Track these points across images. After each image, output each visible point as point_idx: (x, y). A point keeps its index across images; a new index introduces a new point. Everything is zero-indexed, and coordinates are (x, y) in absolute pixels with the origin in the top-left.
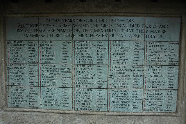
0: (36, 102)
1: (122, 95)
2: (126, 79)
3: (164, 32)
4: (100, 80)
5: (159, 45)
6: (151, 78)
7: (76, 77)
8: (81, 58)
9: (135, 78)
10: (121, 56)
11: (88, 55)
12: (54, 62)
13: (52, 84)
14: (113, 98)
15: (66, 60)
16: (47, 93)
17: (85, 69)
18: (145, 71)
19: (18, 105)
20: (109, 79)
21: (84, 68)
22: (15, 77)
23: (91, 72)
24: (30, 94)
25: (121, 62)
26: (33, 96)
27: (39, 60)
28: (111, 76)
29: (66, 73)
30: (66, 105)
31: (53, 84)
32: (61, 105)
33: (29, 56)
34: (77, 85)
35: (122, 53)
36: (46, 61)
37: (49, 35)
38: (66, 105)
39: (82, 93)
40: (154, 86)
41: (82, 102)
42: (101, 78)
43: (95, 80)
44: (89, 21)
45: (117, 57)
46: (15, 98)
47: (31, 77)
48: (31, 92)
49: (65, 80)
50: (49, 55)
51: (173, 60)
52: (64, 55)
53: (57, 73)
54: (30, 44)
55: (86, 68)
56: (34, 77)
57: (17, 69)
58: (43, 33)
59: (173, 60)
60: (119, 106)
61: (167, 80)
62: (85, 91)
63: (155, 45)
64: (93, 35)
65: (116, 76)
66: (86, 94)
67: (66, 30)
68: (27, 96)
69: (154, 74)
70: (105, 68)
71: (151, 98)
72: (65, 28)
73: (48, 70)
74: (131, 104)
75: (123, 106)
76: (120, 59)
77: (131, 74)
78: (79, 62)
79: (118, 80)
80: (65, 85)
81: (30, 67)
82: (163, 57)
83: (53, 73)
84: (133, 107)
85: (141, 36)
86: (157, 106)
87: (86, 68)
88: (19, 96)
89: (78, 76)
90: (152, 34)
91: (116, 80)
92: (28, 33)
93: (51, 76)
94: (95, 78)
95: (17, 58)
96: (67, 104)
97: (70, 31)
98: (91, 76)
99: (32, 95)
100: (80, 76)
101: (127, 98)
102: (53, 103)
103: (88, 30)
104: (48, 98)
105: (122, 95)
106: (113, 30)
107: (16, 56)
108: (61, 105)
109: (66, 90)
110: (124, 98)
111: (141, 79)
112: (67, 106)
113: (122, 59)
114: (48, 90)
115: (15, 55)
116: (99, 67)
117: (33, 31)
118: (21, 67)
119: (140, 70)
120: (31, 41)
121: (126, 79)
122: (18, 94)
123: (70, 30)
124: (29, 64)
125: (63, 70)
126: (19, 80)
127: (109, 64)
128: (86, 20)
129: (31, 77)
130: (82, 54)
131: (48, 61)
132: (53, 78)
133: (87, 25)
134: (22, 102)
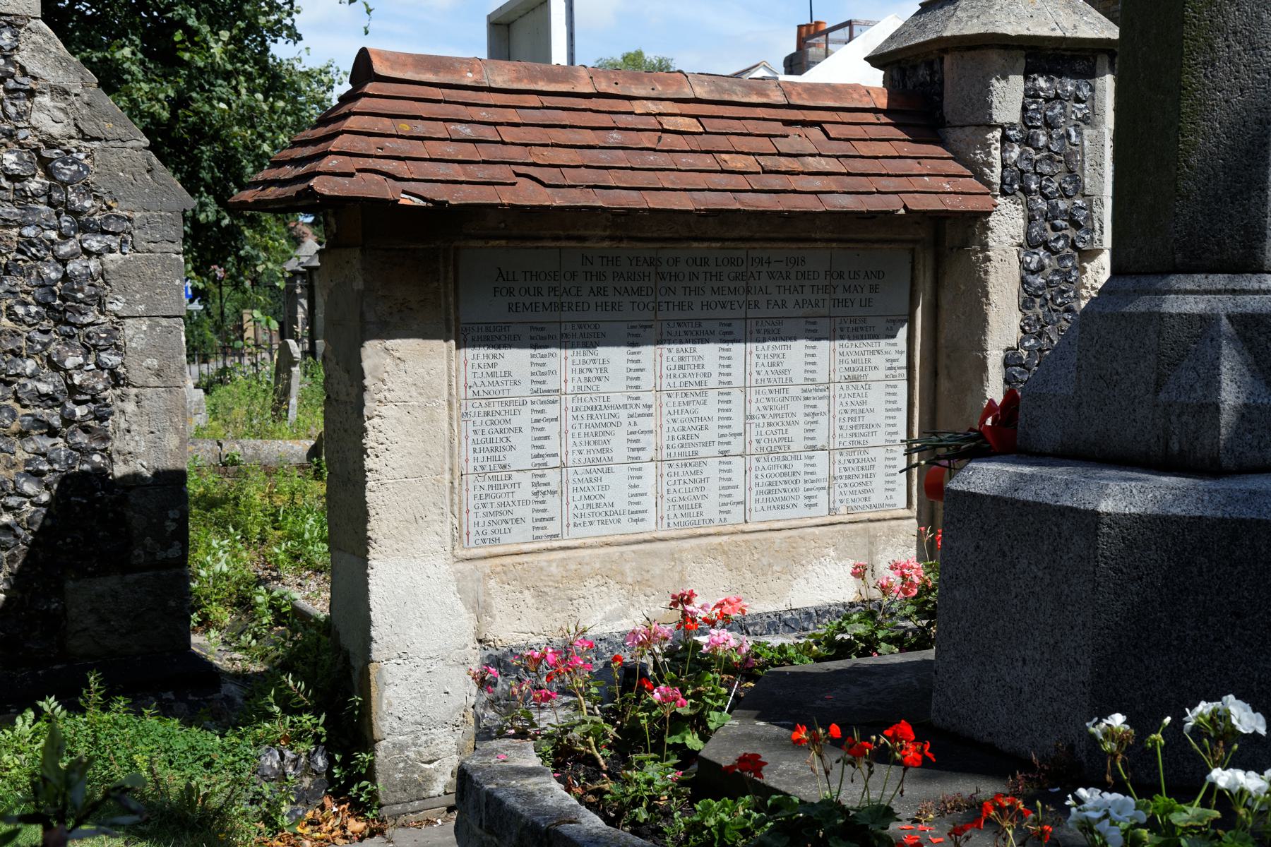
0: (552, 519)
1: (780, 471)
2: (789, 423)
3: (874, 289)
4: (726, 431)
5: (864, 325)
6: (846, 416)
7: (665, 429)
8: (677, 372)
9: (809, 419)
10: (776, 360)
11: (696, 363)
12: (604, 386)
13: (599, 456)
14: (758, 481)
15: (638, 378)
16: (586, 484)
17: (688, 403)
18: (832, 399)
19: (497, 536)
20: (748, 426)
21: (685, 400)
22: (489, 446)
23: (703, 411)
24: (536, 494)
25: (777, 376)
26: (543, 502)
27: (563, 384)
28: (752, 417)
29: (638, 420)
30: (640, 516)
31: (602, 455)
32: (627, 516)
33: (533, 374)
34: (669, 451)
35: (777, 352)
36: (583, 384)
37: (593, 306)
38: (640, 516)
39: (680, 473)
40: (854, 439)
41: (682, 503)
42: (729, 427)
43: (710, 435)
44: (698, 263)
45: (766, 364)
46: (486, 515)
47: (539, 438)
48: (539, 488)
49: (637, 441)
50: (592, 366)
51: (895, 365)
52: (633, 366)
53: (614, 420)
54: (534, 333)
55: (692, 398)
56: (547, 438)
57: (493, 418)
58: (574, 300)
59: (895, 365)
60: (772, 504)
61: (883, 422)
62: (689, 469)
63: (855, 326)
64: (708, 305)
65: (764, 416)
66: (691, 477)
67: (639, 291)
68: (524, 502)
69: (853, 407)
70: (737, 396)
71: (848, 473)
72: (636, 285)
73: (589, 412)
74: (802, 493)
75: (783, 503)
76: (773, 369)
77: (798, 408)
78: (672, 385)
79: (770, 428)
80: (635, 454)
81: (537, 407)
82: (871, 357)
83: (603, 421)
84: (807, 502)
85: (821, 304)
86: (864, 496)
87: (692, 398)
88: (500, 505)
89: (672, 425)
90: (847, 295)
91: (764, 430)
92: (528, 300)
93: (598, 430)
94: (713, 425)
95: (495, 379)
96: (642, 512)
97: (650, 293)
98: (705, 423)
99: (540, 498)
100: (676, 426)
101: (793, 478)
102: (603, 514)
103: (697, 291)
104: (588, 502)
105: (780, 471)
106: (758, 289)
107: (493, 374)
108: (624, 519)
109: (640, 469)
110: (784, 479)
111: (823, 420)
112: (642, 520)
113: (778, 368)
114: (588, 476)
115: (490, 370)
116: (723, 394)
117: (545, 292)
118: (507, 408)
119: (820, 398)
120: (539, 326)
121: (789, 423)
122: (496, 500)
123: (650, 290)
124: (534, 399)
125: (631, 411)
126: (502, 454)
127: (748, 385)
128: (690, 261)
129: (539, 438)
130: (681, 359)
131: (589, 384)
132: (603, 438)
133: (694, 276)
134: (509, 525)
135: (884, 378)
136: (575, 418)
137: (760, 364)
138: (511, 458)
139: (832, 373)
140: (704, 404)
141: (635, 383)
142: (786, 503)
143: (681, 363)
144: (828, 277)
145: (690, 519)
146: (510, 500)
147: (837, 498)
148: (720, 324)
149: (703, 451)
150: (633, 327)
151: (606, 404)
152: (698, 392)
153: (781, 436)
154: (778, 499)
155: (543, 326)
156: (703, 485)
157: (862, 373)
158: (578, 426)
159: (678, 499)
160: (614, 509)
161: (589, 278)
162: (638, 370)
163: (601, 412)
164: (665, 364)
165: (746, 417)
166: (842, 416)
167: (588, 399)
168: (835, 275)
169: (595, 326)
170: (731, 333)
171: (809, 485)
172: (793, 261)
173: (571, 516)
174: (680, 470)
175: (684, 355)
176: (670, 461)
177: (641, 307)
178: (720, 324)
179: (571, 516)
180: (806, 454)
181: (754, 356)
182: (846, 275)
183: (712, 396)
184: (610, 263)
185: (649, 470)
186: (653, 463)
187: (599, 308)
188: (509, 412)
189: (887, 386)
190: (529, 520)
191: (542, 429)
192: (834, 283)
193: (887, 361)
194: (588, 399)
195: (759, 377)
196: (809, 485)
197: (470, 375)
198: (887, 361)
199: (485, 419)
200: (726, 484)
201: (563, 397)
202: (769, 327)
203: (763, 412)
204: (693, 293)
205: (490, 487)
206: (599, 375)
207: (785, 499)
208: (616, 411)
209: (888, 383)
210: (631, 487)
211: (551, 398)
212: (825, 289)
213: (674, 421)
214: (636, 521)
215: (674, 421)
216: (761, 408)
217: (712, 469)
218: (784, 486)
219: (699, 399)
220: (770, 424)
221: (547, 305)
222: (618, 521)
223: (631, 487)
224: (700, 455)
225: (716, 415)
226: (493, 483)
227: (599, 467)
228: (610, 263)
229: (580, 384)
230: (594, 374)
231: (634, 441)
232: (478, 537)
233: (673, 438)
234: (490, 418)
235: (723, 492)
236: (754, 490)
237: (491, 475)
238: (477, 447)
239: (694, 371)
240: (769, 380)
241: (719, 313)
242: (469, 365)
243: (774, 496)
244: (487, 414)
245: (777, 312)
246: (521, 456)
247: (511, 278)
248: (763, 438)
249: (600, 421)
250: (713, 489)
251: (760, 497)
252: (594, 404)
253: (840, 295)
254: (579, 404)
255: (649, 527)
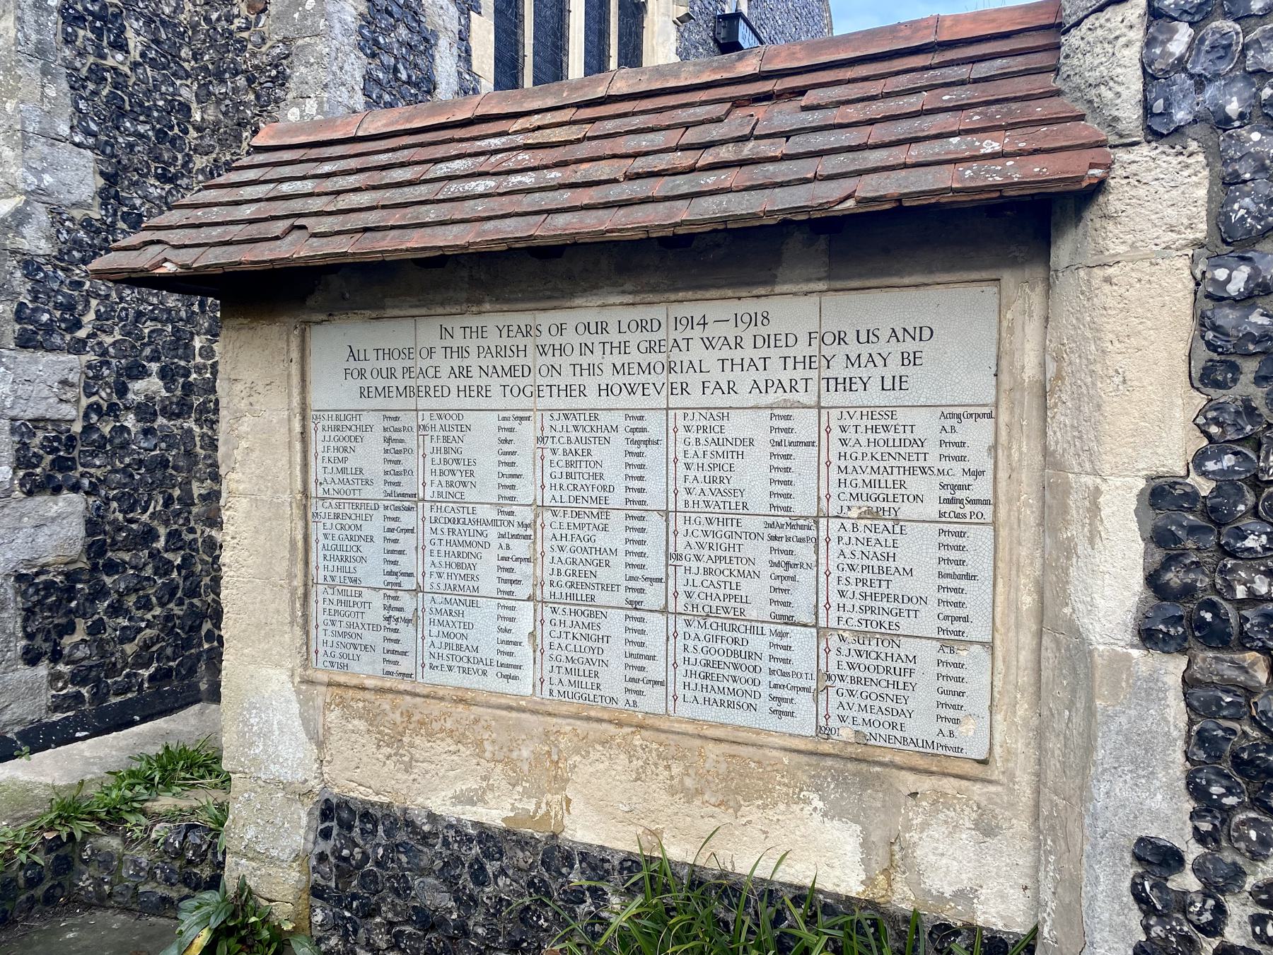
0: (404, 653)
1: (725, 646)
2: (742, 574)
3: (910, 359)
4: (637, 573)
5: (889, 422)
6: (853, 575)
7: (547, 560)
8: (565, 482)
9: (779, 571)
10: (717, 473)
11: (592, 471)
12: (470, 495)
13: (462, 583)
14: (687, 655)
15: (512, 487)
16: (445, 617)
17: (581, 526)
18: (822, 544)
19: (346, 661)
20: (671, 569)
21: (577, 521)
22: (339, 554)
23: (602, 540)
24: (388, 619)
25: (719, 498)
26: (396, 631)
27: (421, 487)
28: (678, 557)
29: (513, 542)
30: (512, 672)
31: (467, 583)
32: (496, 669)
33: (386, 473)
34: (553, 590)
35: (720, 461)
36: (444, 490)
37: (454, 391)
38: (512, 672)
39: (568, 623)
40: (868, 616)
41: (570, 666)
42: (642, 567)
43: (616, 573)
44: (593, 329)
45: (701, 479)
46: (335, 634)
47: (393, 552)
48: (392, 613)
49: (510, 570)
50: (454, 467)
51: (959, 494)
52: (506, 470)
53: (481, 539)
54: (387, 424)
55: (586, 520)
56: (401, 552)
57: (344, 522)
58: (432, 383)
59: (959, 494)
60: (712, 696)
61: (933, 595)
62: (581, 619)
63: (870, 423)
64: (609, 390)
65: (698, 558)
66: (584, 631)
67: (512, 371)
68: (375, 627)
69: (866, 562)
70: (655, 525)
71: (856, 673)
72: (507, 363)
73: (450, 526)
74: (764, 689)
75: (731, 698)
76: (714, 486)
77: (760, 552)
78: (558, 498)
79: (710, 578)
80: (507, 587)
81: (389, 513)
82: (908, 479)
83: (468, 539)
84: (774, 705)
85: (801, 386)
86: (890, 718)
87: (586, 520)
88: (350, 625)
89: (557, 554)
90: (854, 372)
91: (699, 579)
92: (380, 383)
93: (461, 549)
94: (619, 561)
95: (345, 476)
96: (516, 667)
97: (526, 373)
98: (604, 557)
99: (393, 625)
100: (564, 556)
101: (748, 662)
102: (465, 659)
103: (592, 370)
104: (447, 640)
105: (725, 646)
106: (686, 365)
107: (343, 471)
108: (492, 671)
109: (513, 608)
110: (733, 660)
111: (806, 577)
112: (515, 678)
113: (722, 487)
114: (448, 607)
115: (340, 466)
116: (633, 517)
117: (399, 373)
118: (358, 511)
119: (800, 540)
120: (393, 414)
121: (742, 574)
122: (345, 619)
123: (526, 369)
124: (386, 503)
125: (503, 530)
126: (352, 565)
127: (672, 507)
128: (581, 328)
129: (393, 552)
130: (570, 464)
131: (451, 490)
132: (467, 561)
133: (586, 348)
134: (358, 652)
135: (936, 516)
136: (434, 531)
137: (691, 478)
138: (361, 570)
139: (824, 500)
140: (605, 529)
141: (508, 493)
142: (736, 699)
143: (570, 470)
144: (815, 343)
145: (582, 691)
146: (359, 621)
147: (834, 712)
148: (627, 416)
149: (602, 597)
150: (504, 419)
151: (472, 517)
152: (595, 512)
153: (728, 591)
154: (722, 691)
155: (643, 413)
156: (600, 645)
157: (886, 505)
158: (438, 542)
159: (564, 658)
160: (478, 656)
161: (449, 355)
162: (512, 476)
163: (465, 527)
164: (548, 470)
165: (668, 556)
166: (843, 575)
167: (449, 509)
168: (829, 338)
169: (458, 416)
170: (643, 430)
171: (777, 679)
172: (746, 318)
173: (427, 654)
174: (569, 619)
175: (574, 459)
176: (553, 603)
177: (515, 393)
178: (627, 416)
179: (427, 654)
180: (773, 627)
181: (681, 465)
182: (851, 337)
183: (617, 519)
184: (474, 335)
185: (525, 615)
186: (531, 604)
187: (462, 394)
188: (359, 517)
189: (941, 532)
190: (379, 650)
191: (396, 541)
192: (827, 351)
193: (943, 487)
194: (449, 509)
195: (690, 498)
196: (777, 679)
197: (320, 470)
198: (943, 487)
199: (335, 522)
200: (636, 650)
201: (420, 504)
202: (704, 423)
203: (696, 551)
204: (585, 373)
205: (339, 601)
206: (464, 479)
207: (735, 692)
208: (483, 528)
209: (945, 526)
210: (500, 630)
211: (407, 504)
212: (809, 362)
213: (561, 549)
214: (508, 677)
215: (561, 549)
216: (693, 545)
217: (614, 624)
218: (732, 672)
219: (597, 522)
220: (708, 571)
221: (401, 390)
222: (484, 673)
223: (500, 630)
224: (598, 601)
225: (622, 547)
226: (343, 598)
227: (462, 598)
228: (474, 335)
229: (440, 489)
230: (458, 477)
231: (507, 570)
232: (326, 658)
233: (559, 573)
234: (340, 521)
235: (631, 661)
236: (682, 668)
237: (341, 588)
238: (328, 553)
239: (588, 482)
240: (707, 504)
241: (625, 400)
242: (320, 457)
243: (716, 684)
244: (337, 516)
245: (719, 400)
246: (372, 571)
247: (362, 357)
248: (697, 590)
249: (464, 538)
250: (615, 653)
251: (693, 681)
252: (456, 516)
253: (839, 369)
254: (438, 515)
255: (524, 686)
